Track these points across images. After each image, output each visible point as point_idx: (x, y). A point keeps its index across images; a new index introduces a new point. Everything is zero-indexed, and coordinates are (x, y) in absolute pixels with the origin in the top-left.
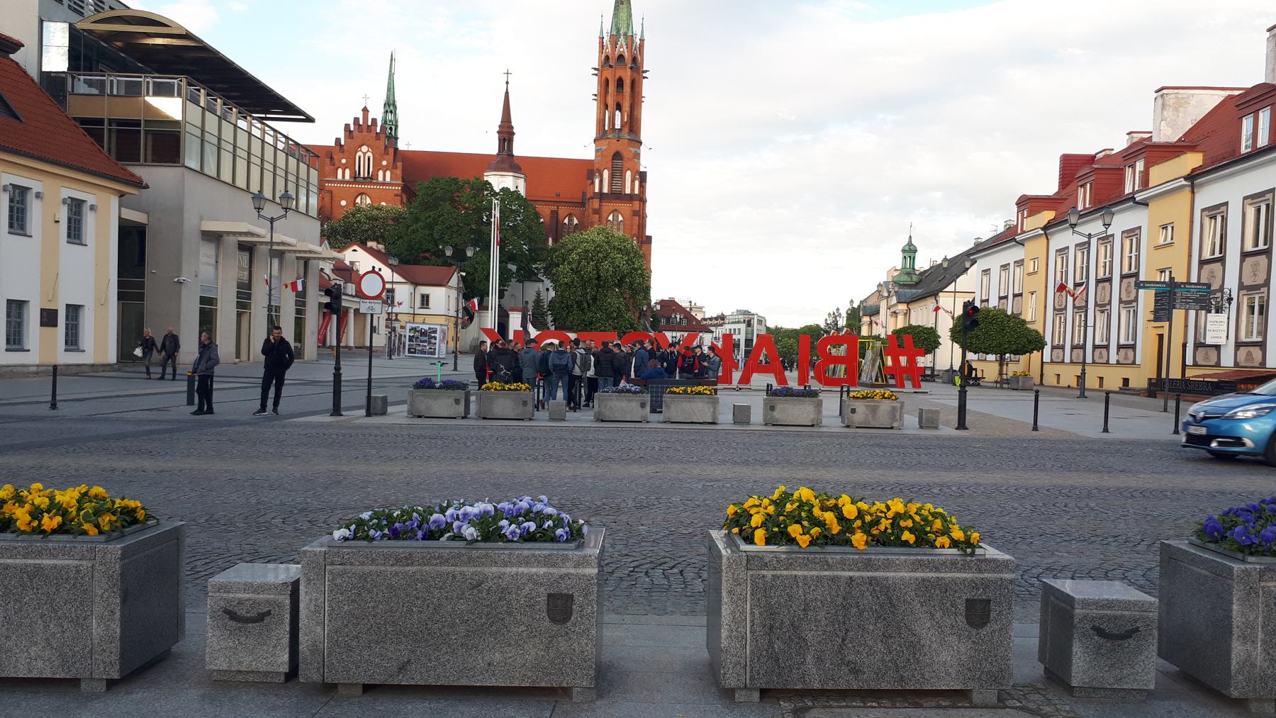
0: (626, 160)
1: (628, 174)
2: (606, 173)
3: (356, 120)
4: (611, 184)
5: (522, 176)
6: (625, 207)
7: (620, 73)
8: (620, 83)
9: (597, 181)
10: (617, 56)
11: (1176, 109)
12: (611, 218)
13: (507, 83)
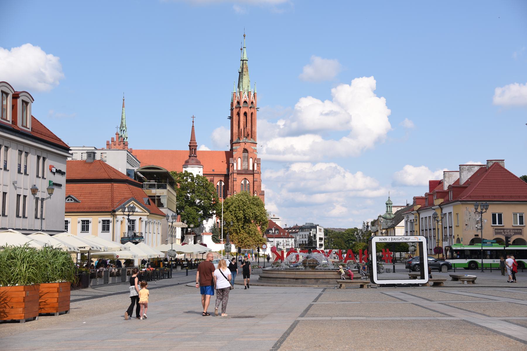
0: (249, 153)
1: (251, 160)
2: (239, 160)
3: (113, 139)
4: (241, 166)
5: (202, 167)
6: (250, 177)
7: (246, 110)
8: (245, 114)
9: (235, 164)
10: (243, 102)
11: (449, 178)
12: (243, 182)
13: (193, 122)
